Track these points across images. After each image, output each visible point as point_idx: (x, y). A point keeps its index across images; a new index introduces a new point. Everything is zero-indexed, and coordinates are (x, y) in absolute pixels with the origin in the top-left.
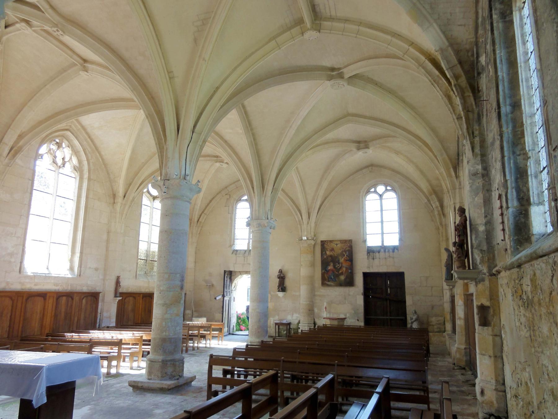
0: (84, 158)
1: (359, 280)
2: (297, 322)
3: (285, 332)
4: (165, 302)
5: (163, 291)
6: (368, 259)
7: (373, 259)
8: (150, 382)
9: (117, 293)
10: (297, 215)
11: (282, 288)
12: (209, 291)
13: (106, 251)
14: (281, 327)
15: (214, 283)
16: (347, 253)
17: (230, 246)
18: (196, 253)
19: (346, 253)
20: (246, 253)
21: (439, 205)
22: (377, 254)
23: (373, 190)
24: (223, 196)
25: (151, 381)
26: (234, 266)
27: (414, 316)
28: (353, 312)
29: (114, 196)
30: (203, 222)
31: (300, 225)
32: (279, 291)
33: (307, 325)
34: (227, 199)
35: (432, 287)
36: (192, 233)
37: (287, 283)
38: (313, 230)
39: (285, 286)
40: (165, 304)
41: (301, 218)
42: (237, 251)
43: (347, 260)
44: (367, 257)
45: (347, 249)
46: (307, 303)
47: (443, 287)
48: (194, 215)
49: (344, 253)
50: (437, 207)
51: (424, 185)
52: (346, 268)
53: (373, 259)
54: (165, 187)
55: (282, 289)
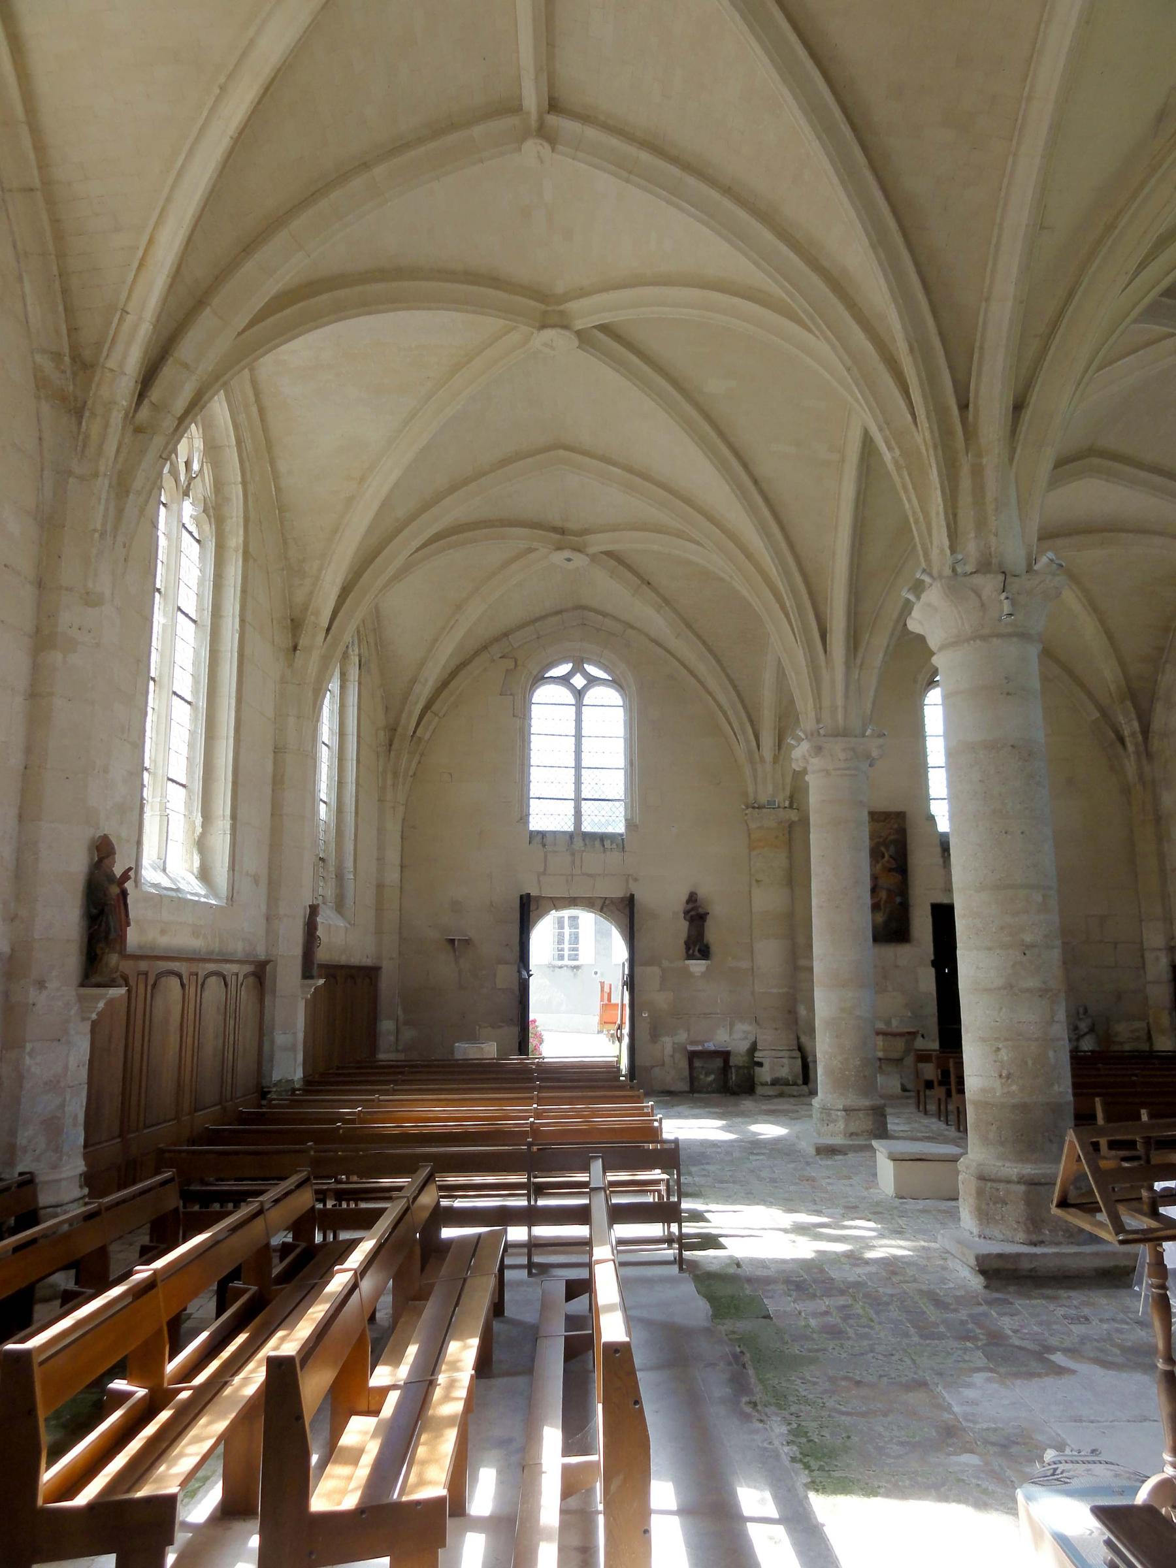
1: (922, 925)
2: (744, 1046)
3: (711, 1078)
4: (1044, 983)
5: (1032, 946)
8: (1035, 1255)
9: (309, 967)
10: (744, 732)
11: (698, 947)
14: (697, 1063)
16: (892, 849)
19: (888, 850)
24: (493, 661)
25: (1038, 1250)
26: (539, 881)
27: (1080, 1019)
28: (909, 1014)
29: (295, 625)
30: (426, 738)
31: (752, 761)
32: (690, 957)
35: (1116, 944)
36: (395, 774)
37: (713, 934)
39: (705, 942)
40: (1047, 991)
41: (754, 744)
42: (542, 834)
43: (890, 870)
45: (892, 837)
46: (781, 991)
47: (1142, 943)
48: (404, 715)
49: (883, 849)
50: (1133, 734)
51: (1107, 674)
52: (889, 891)
54: (1007, 598)
55: (699, 951)
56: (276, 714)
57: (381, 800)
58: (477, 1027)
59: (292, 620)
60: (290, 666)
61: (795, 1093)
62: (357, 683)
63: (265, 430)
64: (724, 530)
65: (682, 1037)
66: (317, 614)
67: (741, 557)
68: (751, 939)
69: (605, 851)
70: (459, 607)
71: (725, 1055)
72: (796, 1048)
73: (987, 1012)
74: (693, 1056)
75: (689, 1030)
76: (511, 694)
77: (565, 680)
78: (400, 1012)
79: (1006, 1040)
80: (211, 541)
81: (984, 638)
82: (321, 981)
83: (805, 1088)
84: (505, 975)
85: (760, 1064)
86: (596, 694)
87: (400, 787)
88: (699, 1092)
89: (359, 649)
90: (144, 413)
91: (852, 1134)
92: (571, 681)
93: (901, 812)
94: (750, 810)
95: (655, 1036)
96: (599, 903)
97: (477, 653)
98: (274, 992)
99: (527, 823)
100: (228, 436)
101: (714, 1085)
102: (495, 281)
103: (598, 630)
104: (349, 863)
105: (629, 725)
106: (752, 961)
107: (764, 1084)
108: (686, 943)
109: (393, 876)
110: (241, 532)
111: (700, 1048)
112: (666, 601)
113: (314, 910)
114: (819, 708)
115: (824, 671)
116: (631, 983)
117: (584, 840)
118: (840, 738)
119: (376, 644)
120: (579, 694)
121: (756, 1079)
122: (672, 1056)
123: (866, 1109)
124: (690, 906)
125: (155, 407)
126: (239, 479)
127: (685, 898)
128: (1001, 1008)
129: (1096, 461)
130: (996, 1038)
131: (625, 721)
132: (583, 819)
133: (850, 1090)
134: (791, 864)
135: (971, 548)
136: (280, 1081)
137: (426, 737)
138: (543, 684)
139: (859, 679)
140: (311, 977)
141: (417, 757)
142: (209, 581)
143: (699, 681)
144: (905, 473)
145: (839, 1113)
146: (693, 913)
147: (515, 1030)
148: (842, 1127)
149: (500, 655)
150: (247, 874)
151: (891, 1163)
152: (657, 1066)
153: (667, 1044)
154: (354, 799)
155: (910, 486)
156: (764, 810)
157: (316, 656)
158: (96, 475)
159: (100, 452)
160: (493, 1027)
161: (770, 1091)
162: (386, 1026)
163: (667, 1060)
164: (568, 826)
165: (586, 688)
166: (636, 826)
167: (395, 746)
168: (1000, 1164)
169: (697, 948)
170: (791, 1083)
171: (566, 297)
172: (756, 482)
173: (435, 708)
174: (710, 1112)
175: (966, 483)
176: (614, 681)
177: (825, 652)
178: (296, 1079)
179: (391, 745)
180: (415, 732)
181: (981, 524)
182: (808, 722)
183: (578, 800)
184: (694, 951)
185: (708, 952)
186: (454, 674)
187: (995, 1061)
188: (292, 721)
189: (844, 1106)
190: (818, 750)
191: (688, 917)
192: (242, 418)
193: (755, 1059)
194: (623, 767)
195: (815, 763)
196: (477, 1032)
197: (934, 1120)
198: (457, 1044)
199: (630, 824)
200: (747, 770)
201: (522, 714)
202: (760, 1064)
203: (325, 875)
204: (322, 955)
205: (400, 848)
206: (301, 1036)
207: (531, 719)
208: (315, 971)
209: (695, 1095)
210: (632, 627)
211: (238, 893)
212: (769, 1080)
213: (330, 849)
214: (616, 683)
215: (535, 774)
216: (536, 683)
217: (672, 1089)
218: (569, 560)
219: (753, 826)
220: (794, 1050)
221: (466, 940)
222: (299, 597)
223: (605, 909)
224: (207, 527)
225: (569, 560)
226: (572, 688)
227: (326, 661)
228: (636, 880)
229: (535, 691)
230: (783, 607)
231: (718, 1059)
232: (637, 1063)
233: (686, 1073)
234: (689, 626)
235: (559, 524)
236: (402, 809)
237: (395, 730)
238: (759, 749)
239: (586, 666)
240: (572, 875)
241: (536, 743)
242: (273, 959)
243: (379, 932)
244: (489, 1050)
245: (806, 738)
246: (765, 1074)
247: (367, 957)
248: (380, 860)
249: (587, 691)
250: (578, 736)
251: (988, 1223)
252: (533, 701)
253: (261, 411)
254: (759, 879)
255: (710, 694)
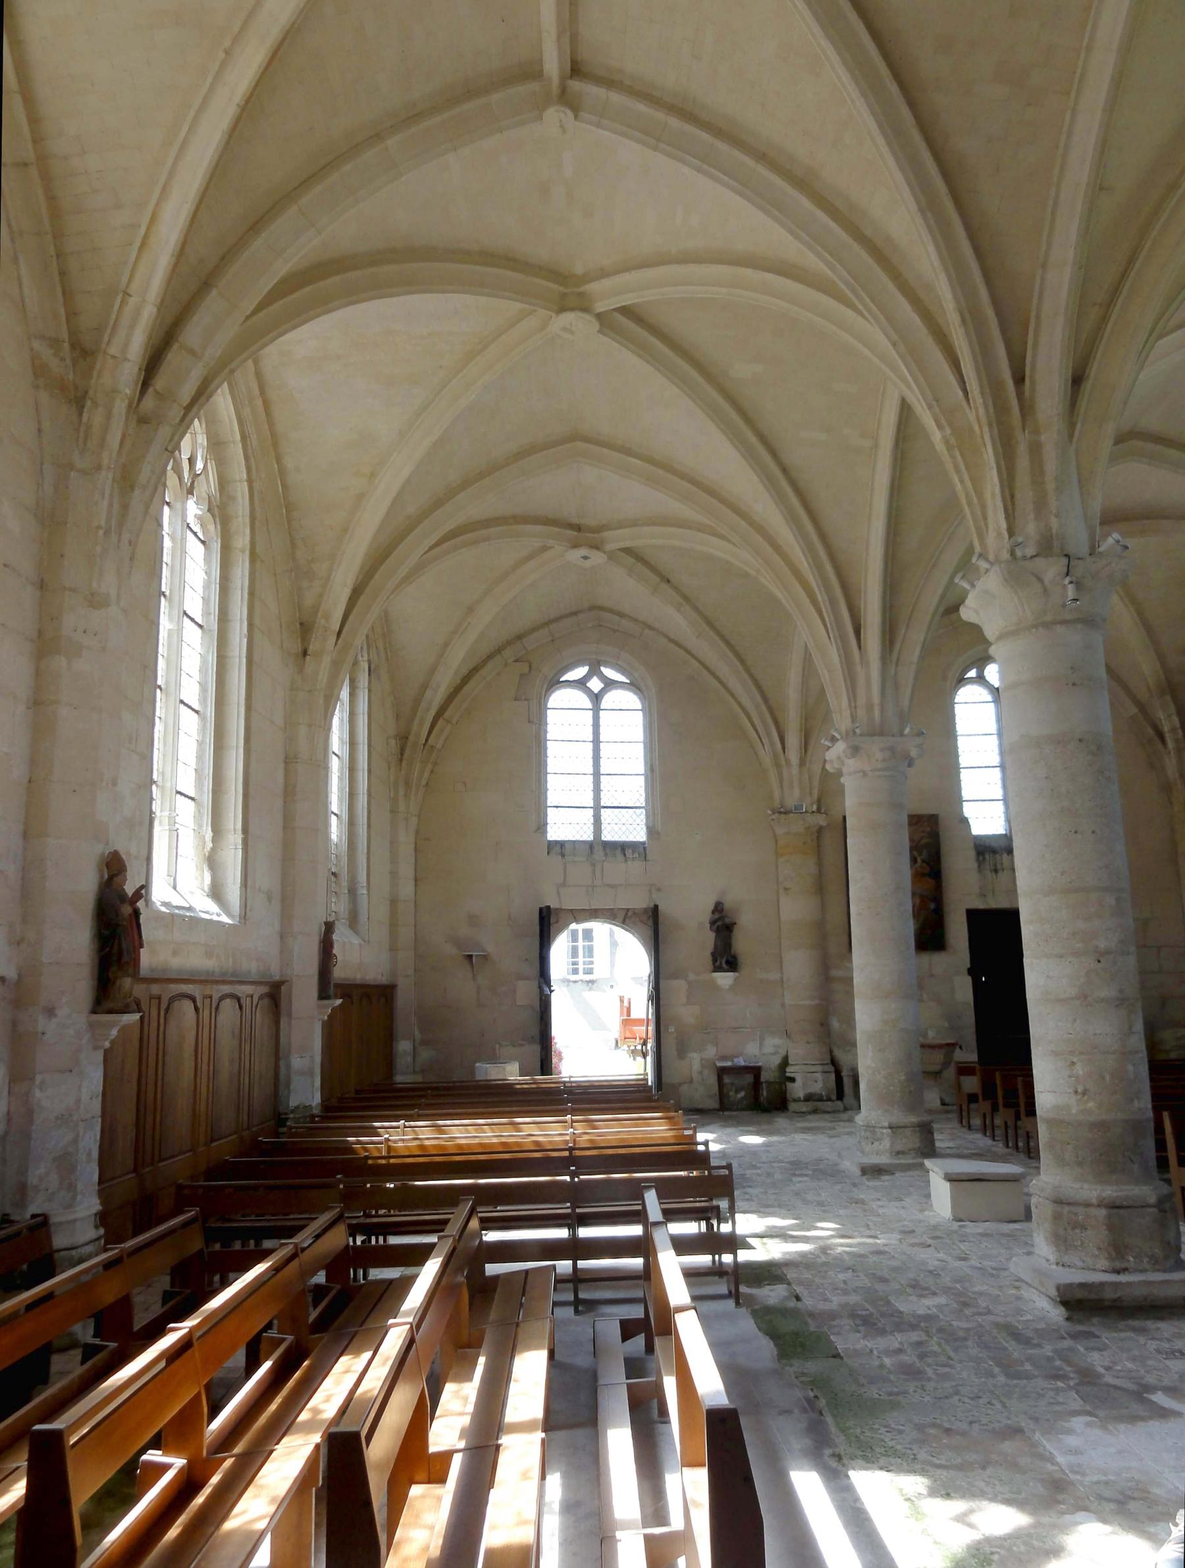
0: (239, 471)
1: (958, 931)
2: (776, 1061)
3: (742, 1094)
5: (1107, 952)
6: (979, 871)
7: (996, 871)
8: (1120, 1283)
9: (325, 985)
10: (769, 734)
12: (474, 978)
13: (285, 828)
14: (727, 1080)
15: (490, 949)
16: (925, 852)
17: (539, 829)
18: (416, 850)
19: (920, 854)
20: (595, 850)
21: (1178, 725)
22: (1005, 856)
23: (972, 673)
25: (1123, 1278)
26: (558, 893)
28: (946, 1025)
29: (305, 629)
30: (439, 746)
31: (777, 765)
32: (717, 969)
33: (819, 1068)
34: (522, 675)
36: (408, 784)
37: (741, 944)
38: (816, 783)
39: (732, 952)
41: (779, 746)
42: (561, 844)
43: (923, 875)
44: (976, 865)
45: (924, 841)
46: (813, 1003)
50: (1173, 730)
53: (996, 871)
55: (727, 962)
56: (286, 723)
57: (393, 811)
58: (497, 1046)
59: (301, 624)
60: (301, 670)
61: (829, 1109)
62: (367, 691)
63: (271, 424)
64: (752, 523)
65: (711, 1052)
66: (327, 617)
67: (769, 549)
68: (780, 949)
69: (626, 861)
70: (470, 610)
71: (756, 1071)
72: (829, 1062)
73: (1060, 1024)
74: (722, 1072)
75: (717, 1045)
76: (526, 700)
77: (581, 684)
78: (417, 1033)
79: (1081, 1053)
80: (216, 541)
81: (1047, 625)
82: (339, 1002)
83: (839, 1103)
84: (526, 991)
85: (792, 1080)
86: (613, 698)
87: (413, 798)
88: (727, 1110)
89: (369, 654)
90: (149, 403)
91: (898, 1153)
92: (588, 685)
93: (934, 815)
94: (777, 815)
95: (682, 1052)
96: (621, 915)
97: (490, 657)
98: (290, 1015)
99: (545, 832)
100: (232, 430)
101: (745, 1102)
102: (510, 261)
103: (615, 631)
104: (362, 877)
105: (649, 727)
106: (782, 973)
107: (796, 1100)
108: (713, 954)
109: (407, 890)
110: (248, 531)
111: (729, 1064)
112: (686, 598)
113: (329, 927)
114: (853, 707)
115: (859, 668)
116: (656, 997)
117: (604, 850)
118: (876, 738)
119: (385, 649)
120: (596, 698)
121: (788, 1095)
122: (701, 1073)
123: (913, 1126)
124: (717, 916)
125: (159, 396)
126: (245, 477)
127: (711, 907)
128: (1075, 1020)
129: (1139, 444)
130: (1071, 1052)
131: (644, 725)
132: (603, 828)
133: (896, 1106)
134: (820, 871)
135: (1031, 528)
136: (297, 1107)
137: (439, 746)
138: (559, 688)
139: (896, 674)
140: (327, 997)
141: (429, 767)
142: (216, 583)
143: (721, 682)
144: (957, 454)
145: (884, 1131)
146: (719, 923)
147: (536, 1048)
148: (888, 1145)
149: (513, 659)
150: (260, 889)
151: (948, 1184)
152: (685, 1083)
153: (695, 1060)
154: (366, 810)
155: (962, 467)
156: (792, 815)
157: (327, 660)
158: (99, 468)
159: (102, 444)
160: (514, 1046)
161: (804, 1107)
162: (403, 1046)
163: (695, 1076)
164: (587, 835)
165: (603, 692)
166: (658, 833)
167: (406, 756)
168: (1077, 1186)
169: (724, 961)
170: (825, 1098)
171: (587, 278)
172: (785, 470)
173: (446, 715)
174: (741, 1131)
175: (1023, 463)
176: (631, 684)
177: (860, 647)
178: (314, 1104)
179: (402, 754)
180: (427, 740)
181: (1040, 505)
182: (842, 721)
183: (597, 808)
184: (721, 963)
185: (736, 964)
186: (465, 680)
187: (1070, 1077)
188: (303, 730)
189: (890, 1124)
190: (855, 750)
191: (715, 927)
192: (247, 412)
193: (788, 1074)
194: (643, 772)
195: (851, 764)
196: (497, 1051)
197: (979, 1136)
198: (477, 1065)
199: (651, 831)
200: (772, 774)
201: (537, 720)
202: (792, 1080)
203: (338, 891)
204: (339, 973)
205: (413, 861)
206: (318, 1059)
207: (546, 724)
208: (332, 991)
209: (726, 1113)
210: (650, 628)
211: (251, 910)
212: (801, 1095)
213: (342, 863)
214: (634, 686)
215: (552, 782)
216: (552, 686)
217: (700, 1106)
218: (585, 558)
219: (780, 831)
220: (827, 1064)
221: (485, 956)
222: (309, 600)
223: (627, 920)
224: (211, 527)
225: (585, 558)
226: (588, 692)
227: (336, 665)
228: (659, 890)
229: (550, 695)
230: (814, 602)
231: (748, 1075)
232: (664, 1079)
233: (715, 1089)
234: (710, 623)
235: (575, 521)
236: (414, 820)
237: (407, 738)
238: (784, 752)
239: (602, 669)
240: (593, 887)
241: (552, 749)
242: (289, 979)
243: (393, 949)
244: (512, 1073)
245: (842, 738)
246: (797, 1090)
247: (382, 975)
248: (394, 874)
249: (606, 693)
250: (596, 742)
251: (1067, 1249)
252: (549, 706)
253: (266, 404)
254: (788, 887)
255: (733, 695)
